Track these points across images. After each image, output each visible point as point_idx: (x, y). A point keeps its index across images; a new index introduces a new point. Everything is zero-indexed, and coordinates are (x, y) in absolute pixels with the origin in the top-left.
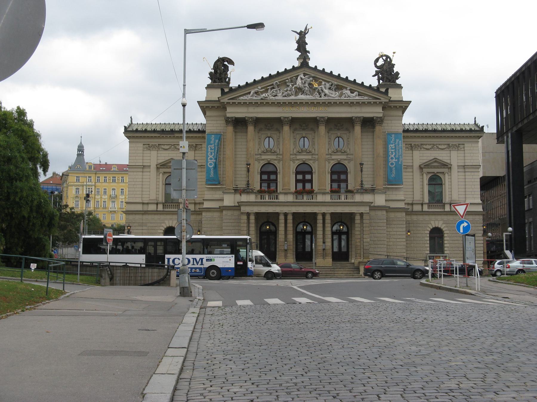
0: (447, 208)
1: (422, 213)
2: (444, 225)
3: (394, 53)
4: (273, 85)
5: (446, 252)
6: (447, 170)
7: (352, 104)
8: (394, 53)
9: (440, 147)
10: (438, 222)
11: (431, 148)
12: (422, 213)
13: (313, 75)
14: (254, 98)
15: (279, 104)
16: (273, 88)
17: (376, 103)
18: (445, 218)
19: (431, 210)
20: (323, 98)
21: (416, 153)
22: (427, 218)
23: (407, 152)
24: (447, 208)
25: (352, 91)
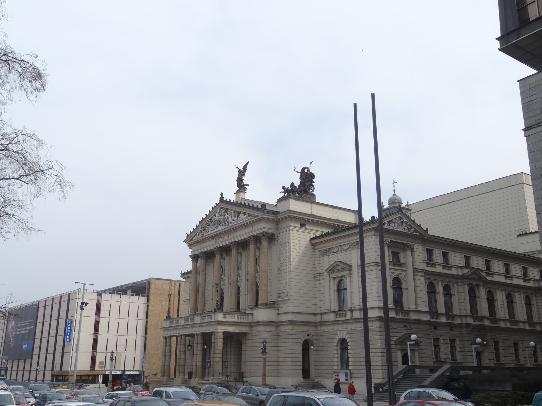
0: (349, 316)
1: (330, 323)
2: (348, 336)
3: (311, 163)
4: (207, 223)
5: (350, 368)
6: (348, 272)
7: (246, 225)
8: (311, 163)
9: (345, 248)
10: (342, 332)
11: (337, 251)
12: (330, 323)
13: (225, 207)
14: (199, 236)
15: (212, 237)
16: (209, 225)
17: (256, 220)
18: (349, 326)
19: (338, 319)
20: (230, 225)
21: (326, 258)
22: (335, 327)
23: (321, 259)
24: (349, 316)
25: (245, 213)
